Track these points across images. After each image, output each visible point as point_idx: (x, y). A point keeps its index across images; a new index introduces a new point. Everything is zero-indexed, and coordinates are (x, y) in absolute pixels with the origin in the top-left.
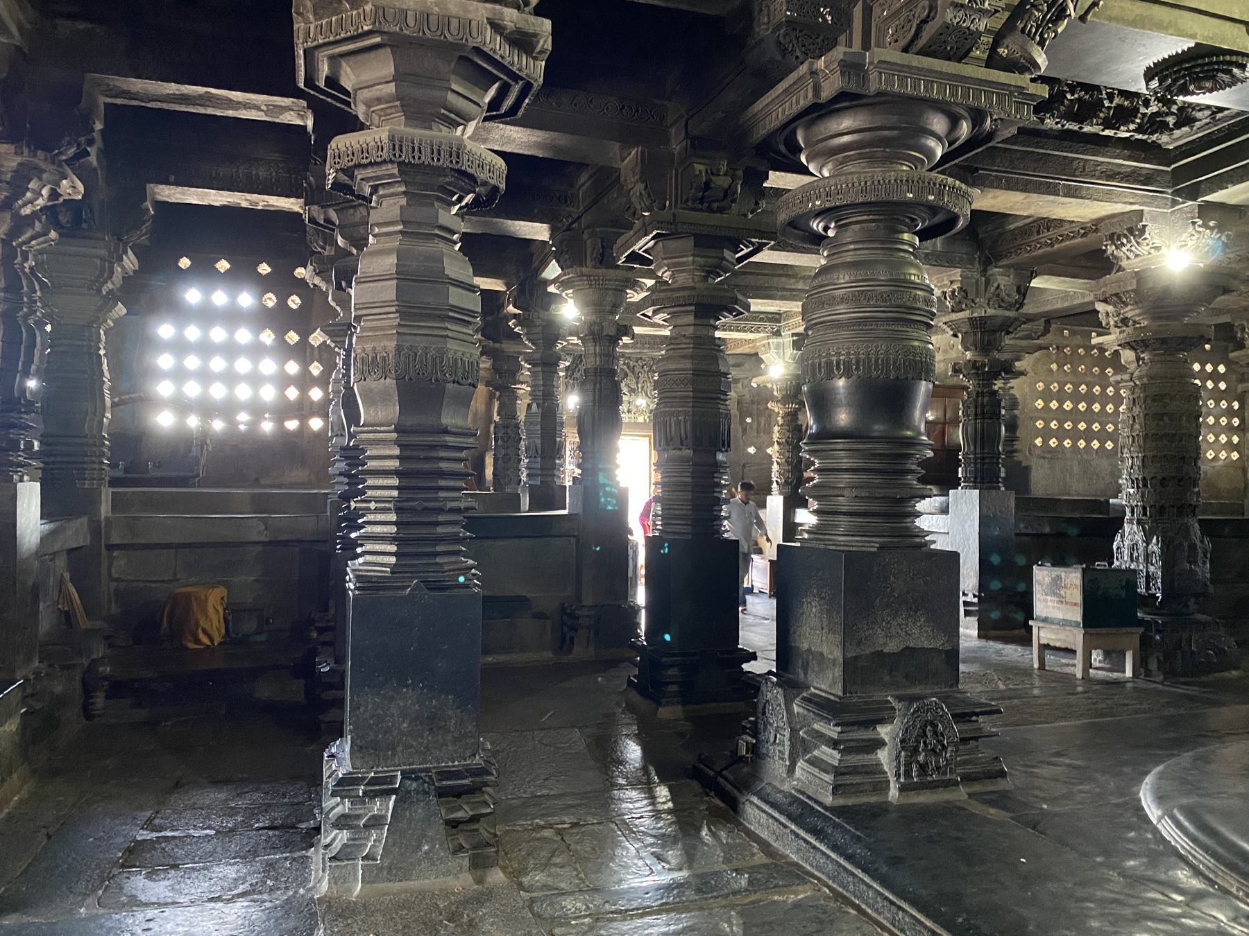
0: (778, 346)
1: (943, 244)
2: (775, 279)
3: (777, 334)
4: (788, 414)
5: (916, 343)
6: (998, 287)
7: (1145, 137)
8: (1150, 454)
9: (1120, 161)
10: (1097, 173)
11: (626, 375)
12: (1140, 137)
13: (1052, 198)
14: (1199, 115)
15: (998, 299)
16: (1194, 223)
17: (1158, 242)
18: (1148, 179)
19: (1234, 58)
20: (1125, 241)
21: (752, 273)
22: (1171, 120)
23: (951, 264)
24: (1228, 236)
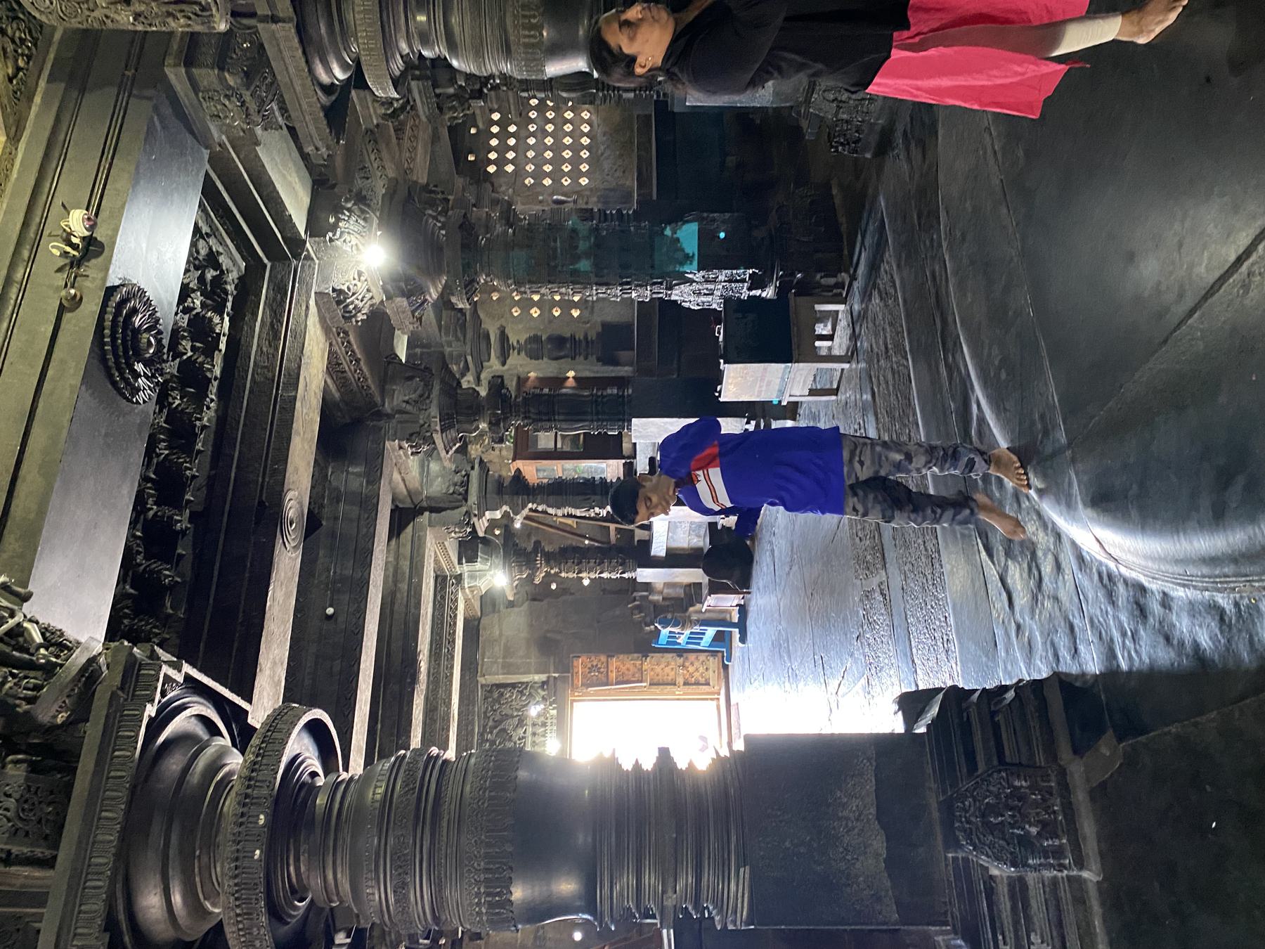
0: (472, 577)
1: (357, 465)
2: (396, 616)
3: (459, 578)
4: (548, 562)
5: (468, 788)
6: (407, 402)
7: (230, 298)
8: (594, 279)
9: (258, 324)
10: (271, 351)
11: (504, 730)
12: (229, 305)
13: (298, 404)
14: (203, 252)
15: (423, 399)
16: (331, 240)
17: (353, 273)
18: (280, 290)
19: (108, 324)
20: (351, 307)
21: (391, 627)
22: (211, 273)
23: (380, 454)
24: (347, 200)
